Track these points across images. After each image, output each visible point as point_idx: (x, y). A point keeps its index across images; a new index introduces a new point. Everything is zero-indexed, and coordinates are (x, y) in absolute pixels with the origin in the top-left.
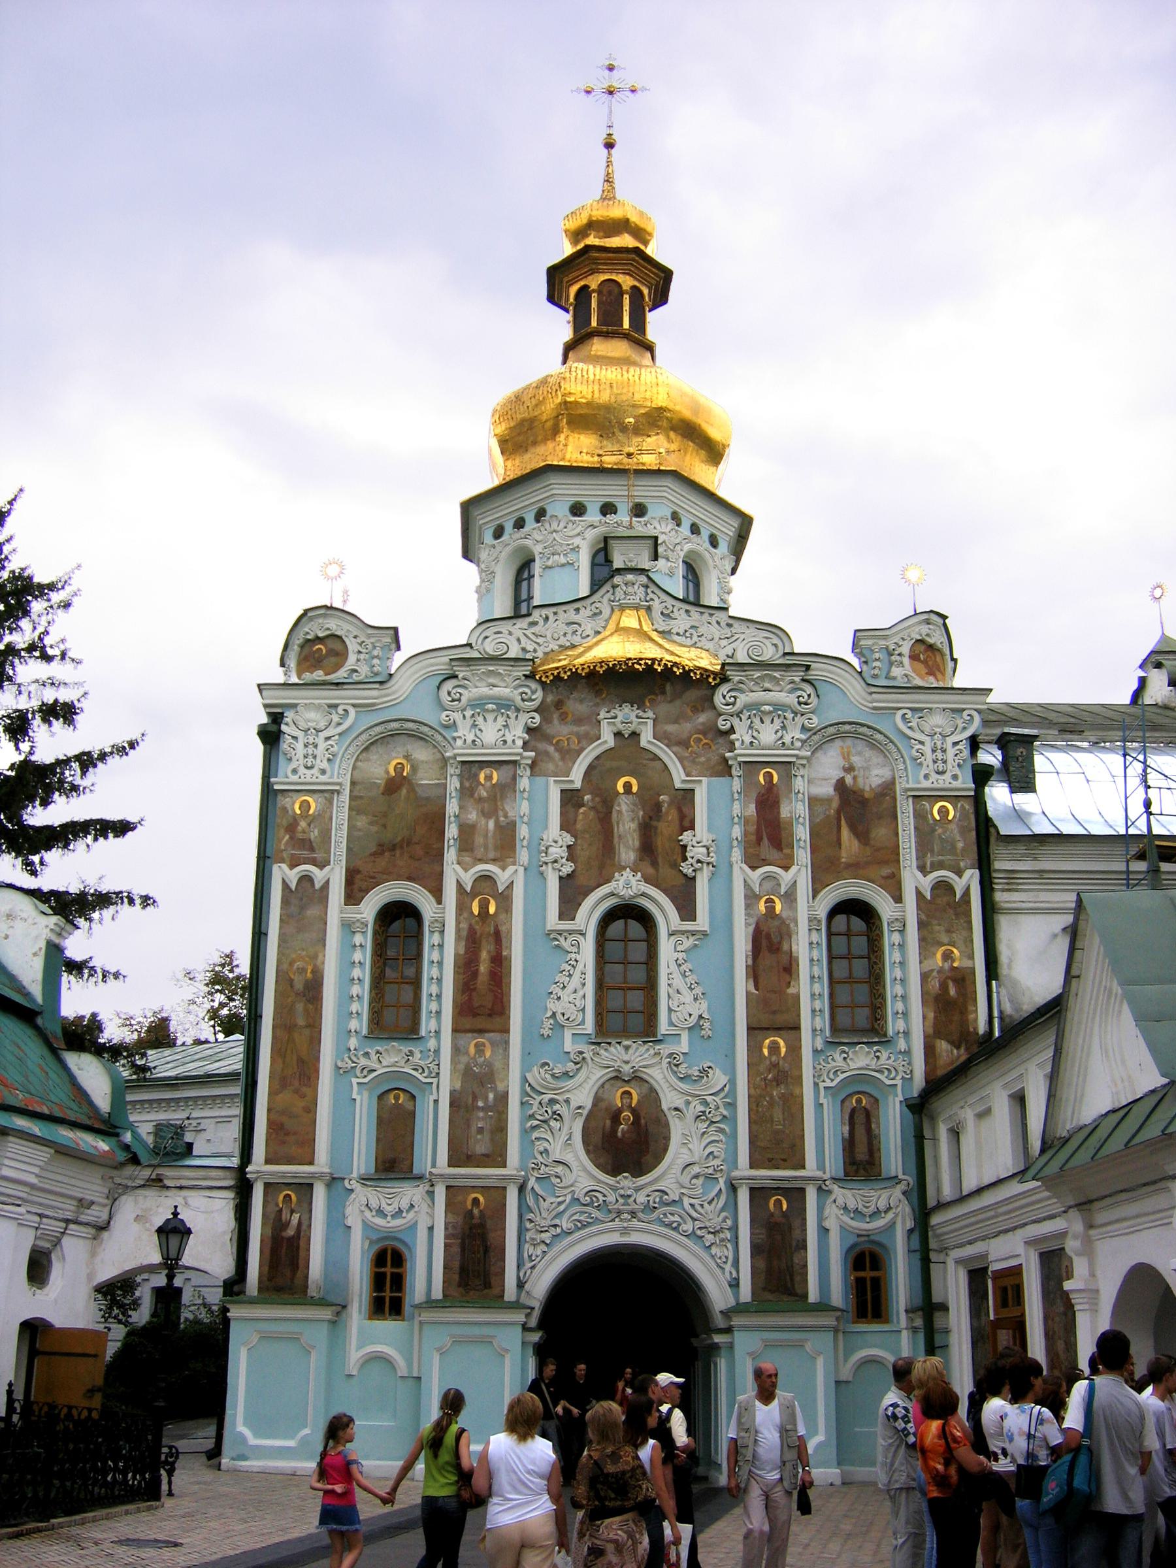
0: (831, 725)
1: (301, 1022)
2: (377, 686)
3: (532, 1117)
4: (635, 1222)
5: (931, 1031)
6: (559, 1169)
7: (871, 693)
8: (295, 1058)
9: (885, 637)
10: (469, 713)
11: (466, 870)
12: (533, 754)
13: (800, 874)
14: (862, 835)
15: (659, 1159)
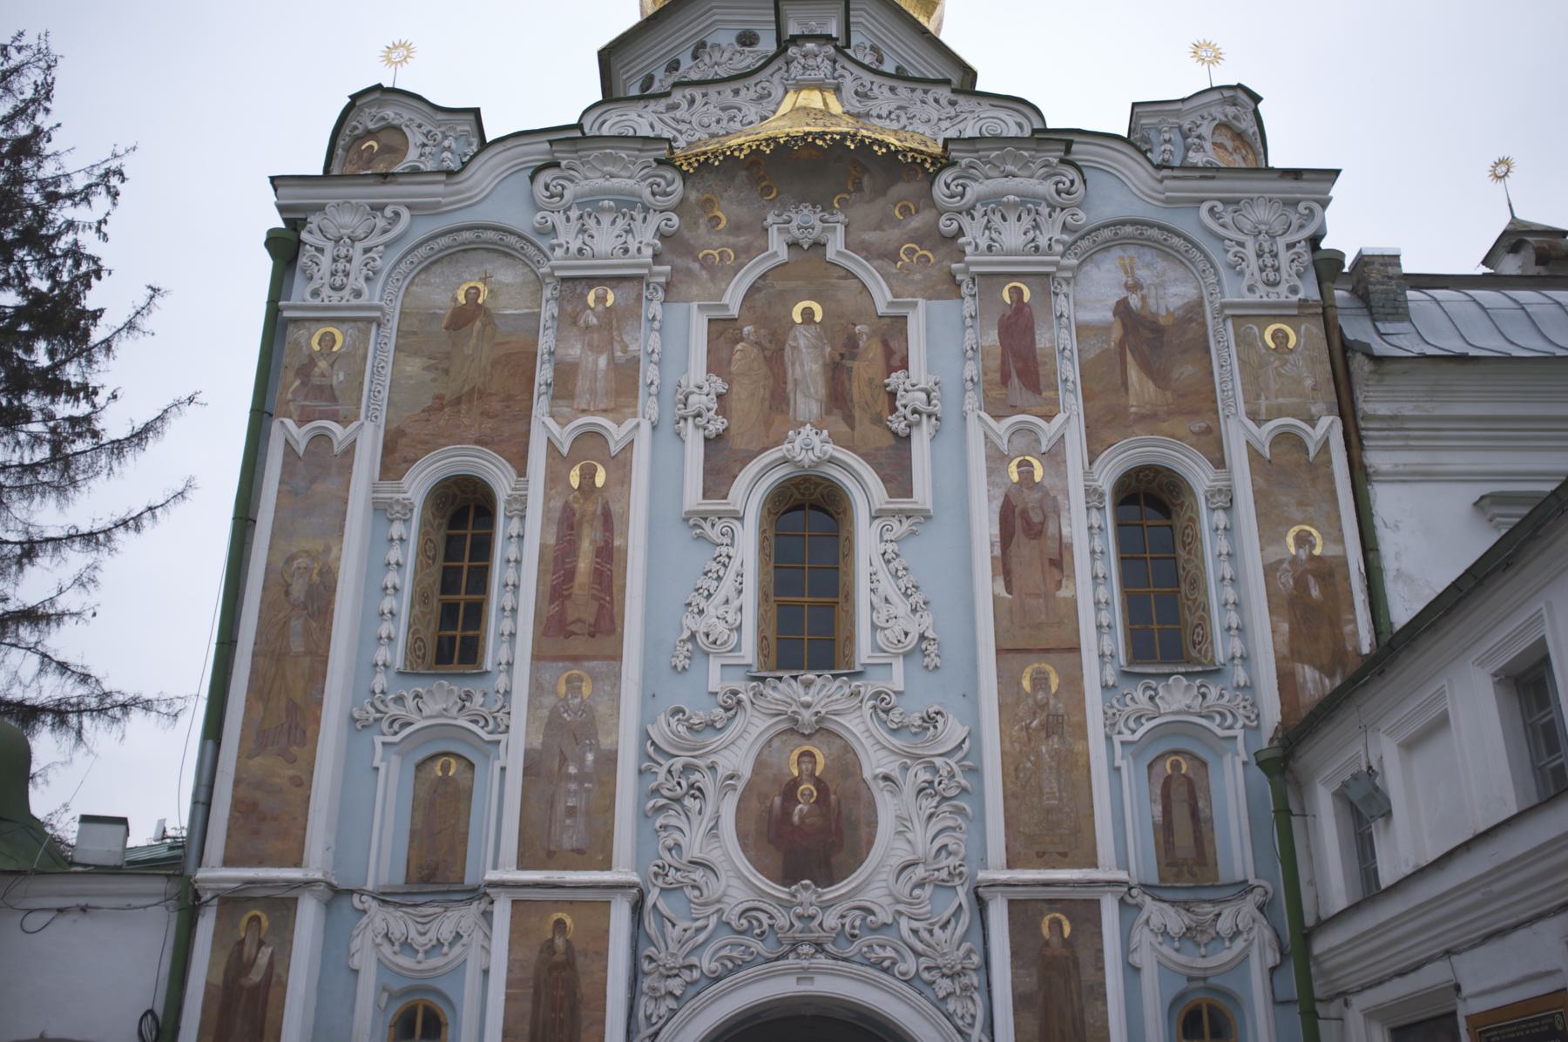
0: (1106, 226)
1: (297, 645)
2: (443, 178)
3: (656, 792)
4: (822, 961)
5: (1285, 651)
6: (698, 875)
7: (1161, 181)
9: (1177, 113)
10: (574, 214)
11: (563, 426)
12: (668, 268)
13: (1069, 423)
15: (858, 860)
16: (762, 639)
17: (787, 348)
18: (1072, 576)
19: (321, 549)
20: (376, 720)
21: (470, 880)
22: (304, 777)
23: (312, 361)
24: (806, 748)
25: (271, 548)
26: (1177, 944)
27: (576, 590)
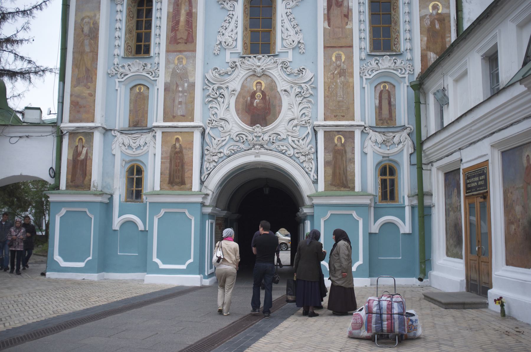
3: (209, 96)
4: (263, 150)
5: (425, 47)
6: (223, 123)
8: (84, 69)
16: (245, 43)
19: (93, 15)
20: (116, 74)
21: (149, 126)
22: (93, 93)
24: (258, 81)
25: (76, 15)
26: (380, 146)
27: (180, 28)
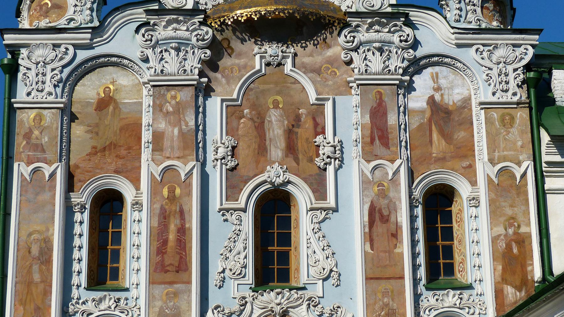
5: (499, 279)
14: (446, 136)
17: (266, 122)
18: (401, 242)
19: (44, 229)
23: (31, 132)
27: (169, 250)
